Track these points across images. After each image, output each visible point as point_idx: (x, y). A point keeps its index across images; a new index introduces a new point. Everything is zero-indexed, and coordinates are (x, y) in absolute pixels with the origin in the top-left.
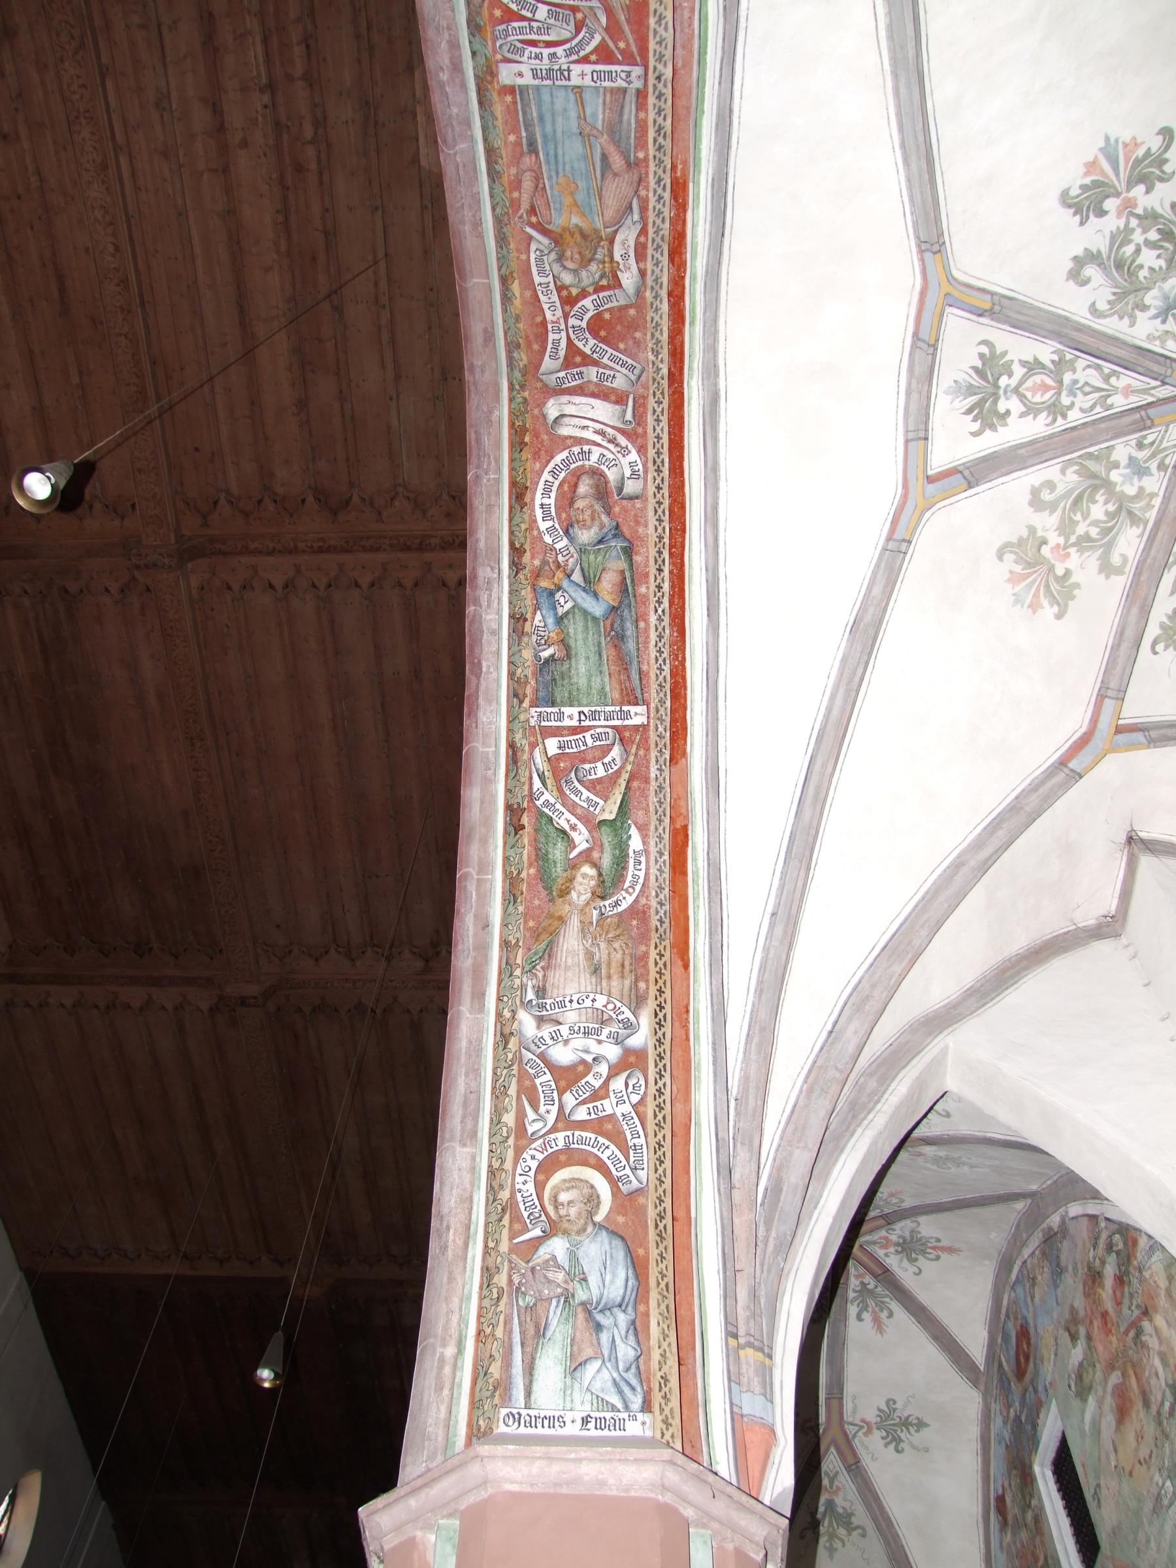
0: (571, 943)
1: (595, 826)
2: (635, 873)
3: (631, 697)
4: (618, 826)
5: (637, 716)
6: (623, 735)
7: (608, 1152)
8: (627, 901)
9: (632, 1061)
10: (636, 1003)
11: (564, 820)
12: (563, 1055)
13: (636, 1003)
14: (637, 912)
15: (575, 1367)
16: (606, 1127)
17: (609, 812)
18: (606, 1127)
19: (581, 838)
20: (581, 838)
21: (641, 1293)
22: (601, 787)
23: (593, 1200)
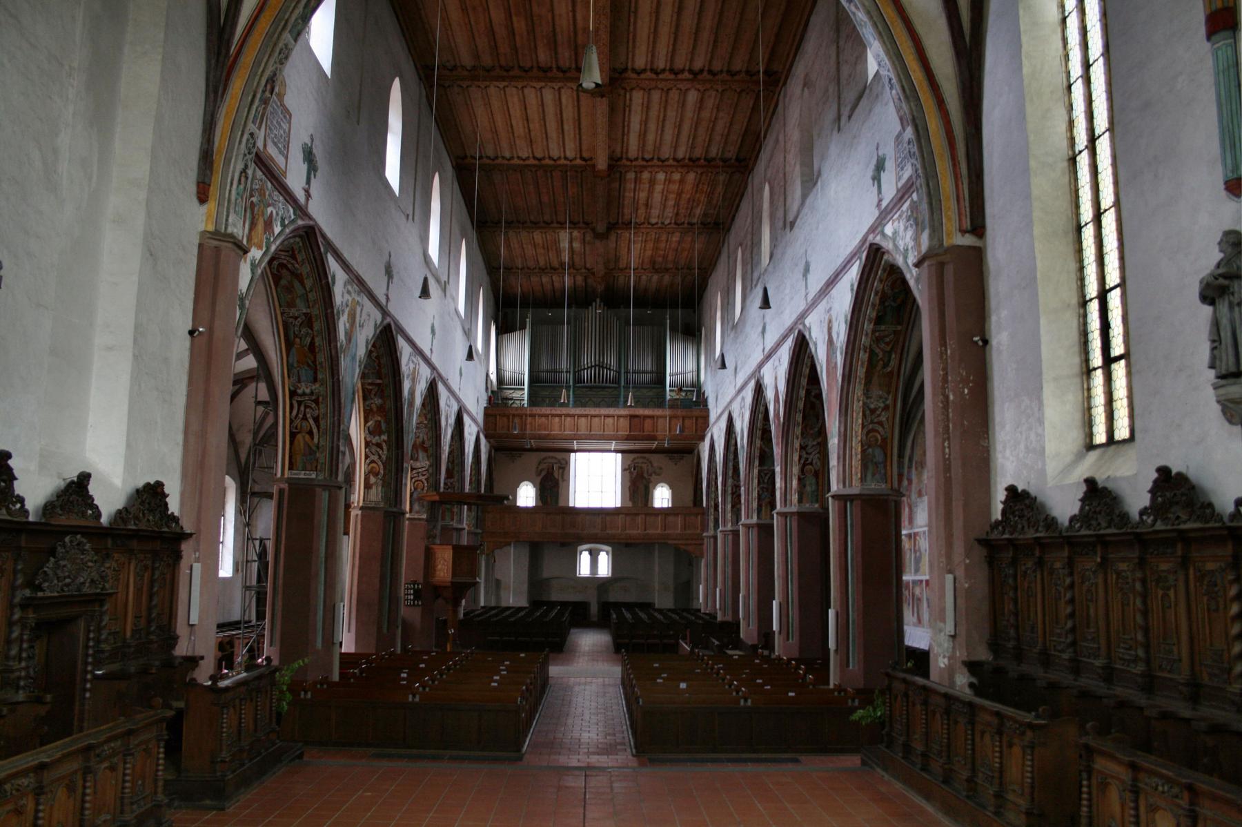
0: (875, 378)
1: (884, 352)
2: (892, 363)
3: (899, 323)
4: (890, 353)
5: (899, 328)
6: (895, 332)
7: (880, 429)
8: (889, 369)
9: (886, 408)
10: (888, 393)
11: (877, 350)
12: (872, 406)
13: (888, 393)
14: (891, 372)
15: (873, 475)
16: (881, 423)
17: (888, 349)
18: (881, 423)
19: (881, 355)
20: (881, 355)
21: (886, 461)
22: (887, 344)
23: (877, 440)
